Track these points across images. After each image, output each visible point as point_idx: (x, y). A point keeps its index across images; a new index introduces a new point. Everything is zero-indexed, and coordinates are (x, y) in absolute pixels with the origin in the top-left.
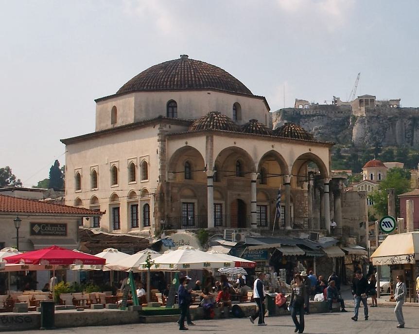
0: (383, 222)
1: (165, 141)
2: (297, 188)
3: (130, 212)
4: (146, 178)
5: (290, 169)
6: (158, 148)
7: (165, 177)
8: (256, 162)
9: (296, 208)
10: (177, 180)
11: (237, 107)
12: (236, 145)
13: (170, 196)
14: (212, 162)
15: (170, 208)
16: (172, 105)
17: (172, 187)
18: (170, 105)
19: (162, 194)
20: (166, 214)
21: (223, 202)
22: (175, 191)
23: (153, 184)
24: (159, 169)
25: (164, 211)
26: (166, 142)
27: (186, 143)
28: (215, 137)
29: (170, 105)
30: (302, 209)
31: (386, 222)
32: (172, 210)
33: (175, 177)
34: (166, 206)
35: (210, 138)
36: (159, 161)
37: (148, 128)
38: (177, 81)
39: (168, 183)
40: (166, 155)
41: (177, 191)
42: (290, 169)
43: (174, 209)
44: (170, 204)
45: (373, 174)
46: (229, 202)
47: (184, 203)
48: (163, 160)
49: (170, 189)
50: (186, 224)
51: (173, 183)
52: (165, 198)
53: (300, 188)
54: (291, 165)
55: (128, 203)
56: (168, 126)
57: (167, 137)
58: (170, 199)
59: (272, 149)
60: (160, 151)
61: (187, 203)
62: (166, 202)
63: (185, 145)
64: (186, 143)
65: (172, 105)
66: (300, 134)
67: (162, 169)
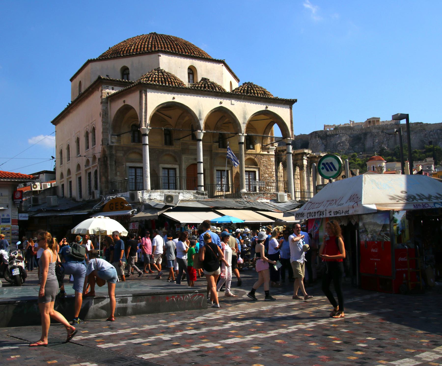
0: (323, 164)
1: (107, 103)
2: (262, 153)
3: (87, 180)
4: (95, 144)
5: (243, 128)
6: (101, 111)
7: (108, 141)
8: (201, 119)
9: (261, 173)
10: (122, 143)
11: (192, 71)
12: (175, 100)
13: (114, 160)
14: (146, 118)
15: (114, 172)
16: (125, 71)
17: (116, 150)
18: (125, 73)
19: (106, 158)
20: (109, 178)
21: (176, 166)
22: (120, 154)
23: (98, 149)
24: (103, 132)
25: (108, 177)
26: (109, 103)
27: (124, 102)
28: (148, 90)
29: (125, 73)
30: (268, 174)
31: (327, 163)
32: (116, 174)
33: (119, 141)
34: (109, 170)
35: (143, 92)
36: (102, 124)
37: (95, 92)
38: (133, 50)
39: (111, 147)
40: (109, 117)
41: (122, 155)
42: (243, 128)
43: (118, 174)
44: (114, 168)
45: (375, 166)
46: (184, 166)
47: (131, 167)
48: (105, 122)
49: (114, 152)
50: (134, 189)
51: (118, 146)
52: (109, 162)
53: (266, 153)
54: (244, 123)
55: (86, 171)
56: (110, 87)
57: (109, 99)
58: (114, 163)
59: (219, 105)
60: (102, 114)
61: (136, 168)
62: (109, 165)
63: (123, 104)
64: (124, 102)
65: (125, 71)
66: (256, 91)
67: (105, 131)
